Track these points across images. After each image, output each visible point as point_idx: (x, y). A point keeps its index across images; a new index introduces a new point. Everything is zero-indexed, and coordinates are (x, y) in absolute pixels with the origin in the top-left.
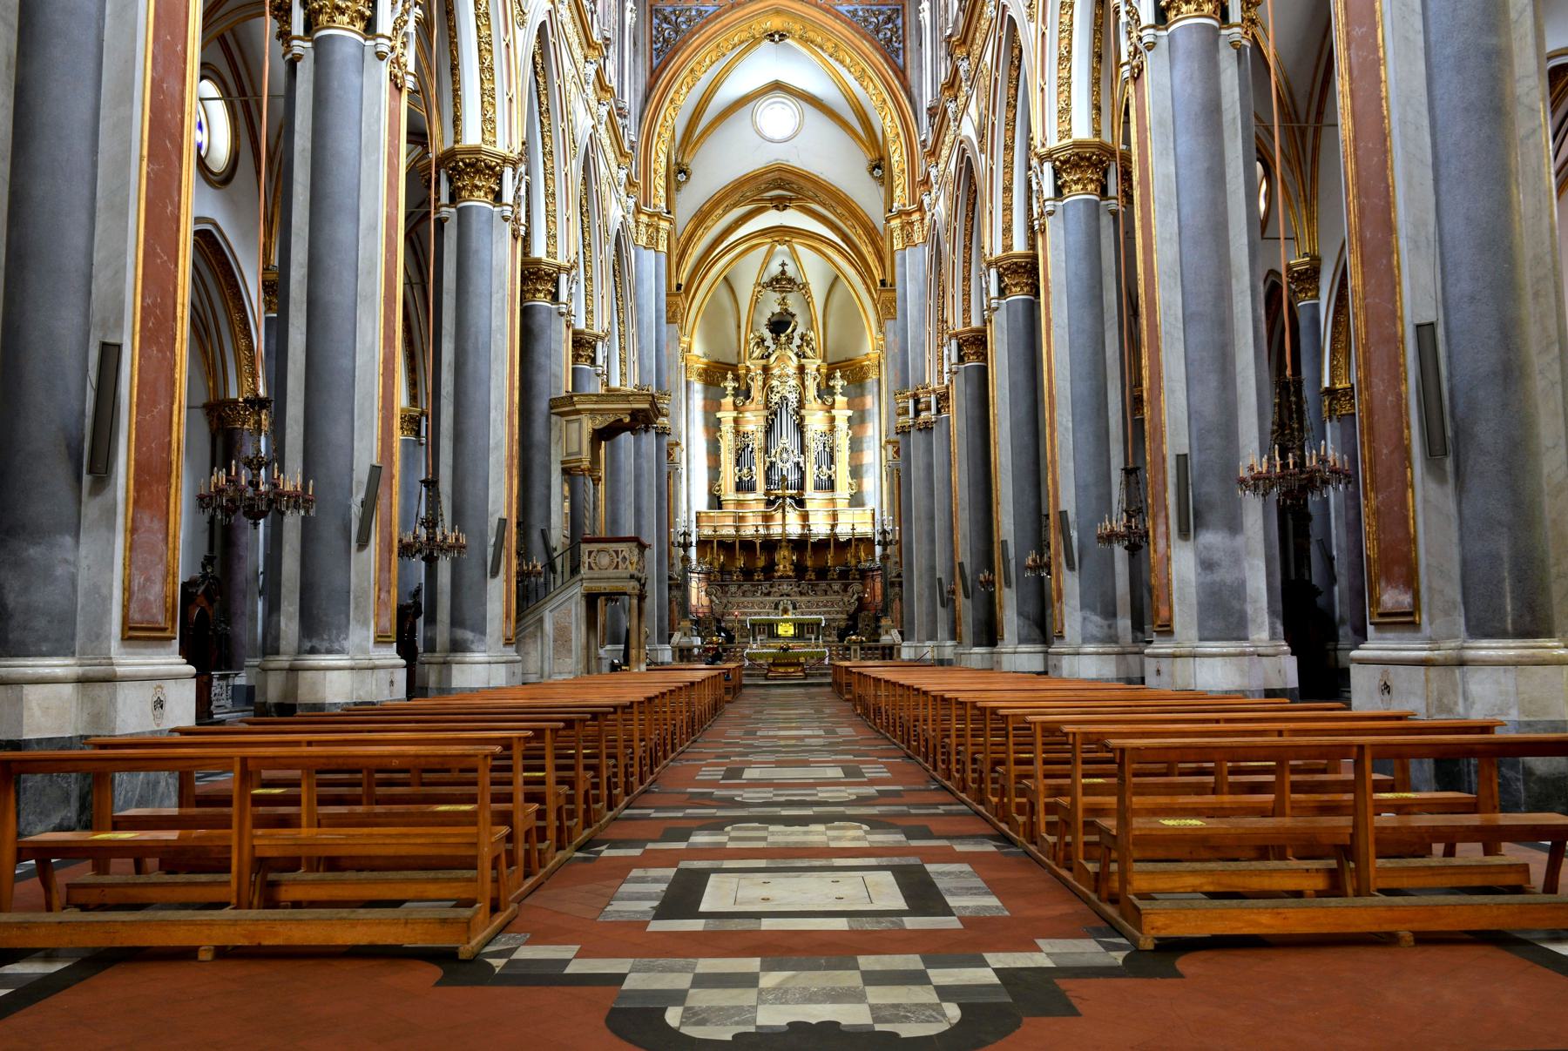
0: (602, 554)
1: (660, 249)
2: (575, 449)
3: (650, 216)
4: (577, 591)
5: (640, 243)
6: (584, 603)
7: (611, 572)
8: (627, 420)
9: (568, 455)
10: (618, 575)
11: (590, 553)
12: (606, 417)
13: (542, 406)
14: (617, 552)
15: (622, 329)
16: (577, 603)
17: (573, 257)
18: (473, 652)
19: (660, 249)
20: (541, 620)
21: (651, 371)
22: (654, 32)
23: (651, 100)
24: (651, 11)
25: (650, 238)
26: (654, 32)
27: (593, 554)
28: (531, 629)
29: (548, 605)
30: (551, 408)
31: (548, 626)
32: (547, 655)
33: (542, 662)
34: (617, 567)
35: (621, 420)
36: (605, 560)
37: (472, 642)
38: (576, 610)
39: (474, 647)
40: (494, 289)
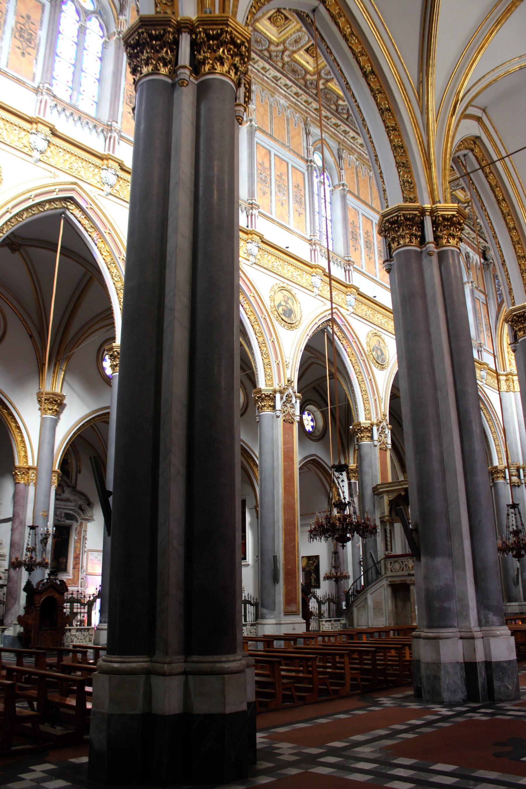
0: (396, 564)
1: (516, 390)
2: (383, 512)
3: (506, 375)
4: (385, 583)
5: (502, 390)
6: (389, 589)
7: (400, 573)
8: (403, 493)
9: (382, 514)
10: (403, 574)
11: (391, 563)
12: (394, 493)
13: (369, 491)
14: (402, 562)
15: (495, 436)
16: (384, 589)
17: (380, 417)
18: (267, 619)
19: (516, 390)
20: (366, 598)
21: (518, 454)
22: (497, 286)
23: (499, 319)
24: (494, 277)
25: (509, 386)
26: (497, 286)
27: (392, 564)
28: (363, 603)
29: (369, 591)
30: (374, 492)
31: (370, 602)
32: (370, 616)
33: (368, 619)
34: (403, 570)
35: (400, 495)
36: (397, 566)
37: (266, 614)
38: (384, 593)
39: (267, 617)
40: (275, 450)
